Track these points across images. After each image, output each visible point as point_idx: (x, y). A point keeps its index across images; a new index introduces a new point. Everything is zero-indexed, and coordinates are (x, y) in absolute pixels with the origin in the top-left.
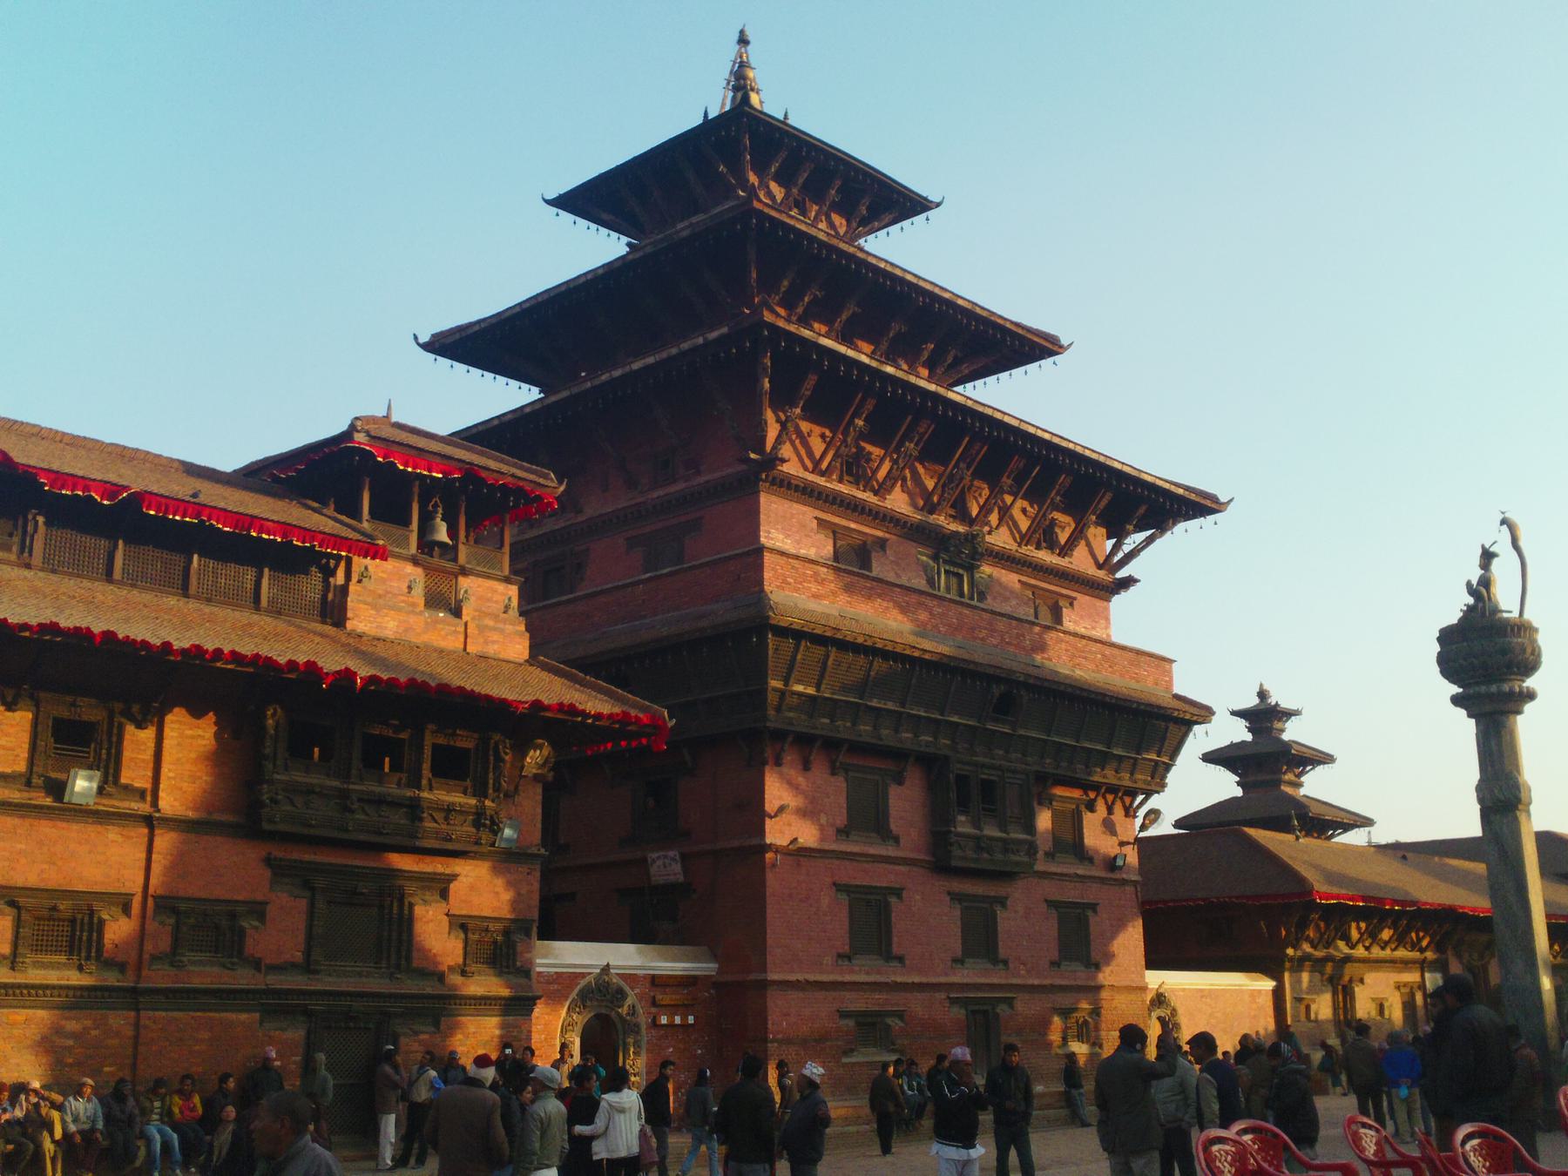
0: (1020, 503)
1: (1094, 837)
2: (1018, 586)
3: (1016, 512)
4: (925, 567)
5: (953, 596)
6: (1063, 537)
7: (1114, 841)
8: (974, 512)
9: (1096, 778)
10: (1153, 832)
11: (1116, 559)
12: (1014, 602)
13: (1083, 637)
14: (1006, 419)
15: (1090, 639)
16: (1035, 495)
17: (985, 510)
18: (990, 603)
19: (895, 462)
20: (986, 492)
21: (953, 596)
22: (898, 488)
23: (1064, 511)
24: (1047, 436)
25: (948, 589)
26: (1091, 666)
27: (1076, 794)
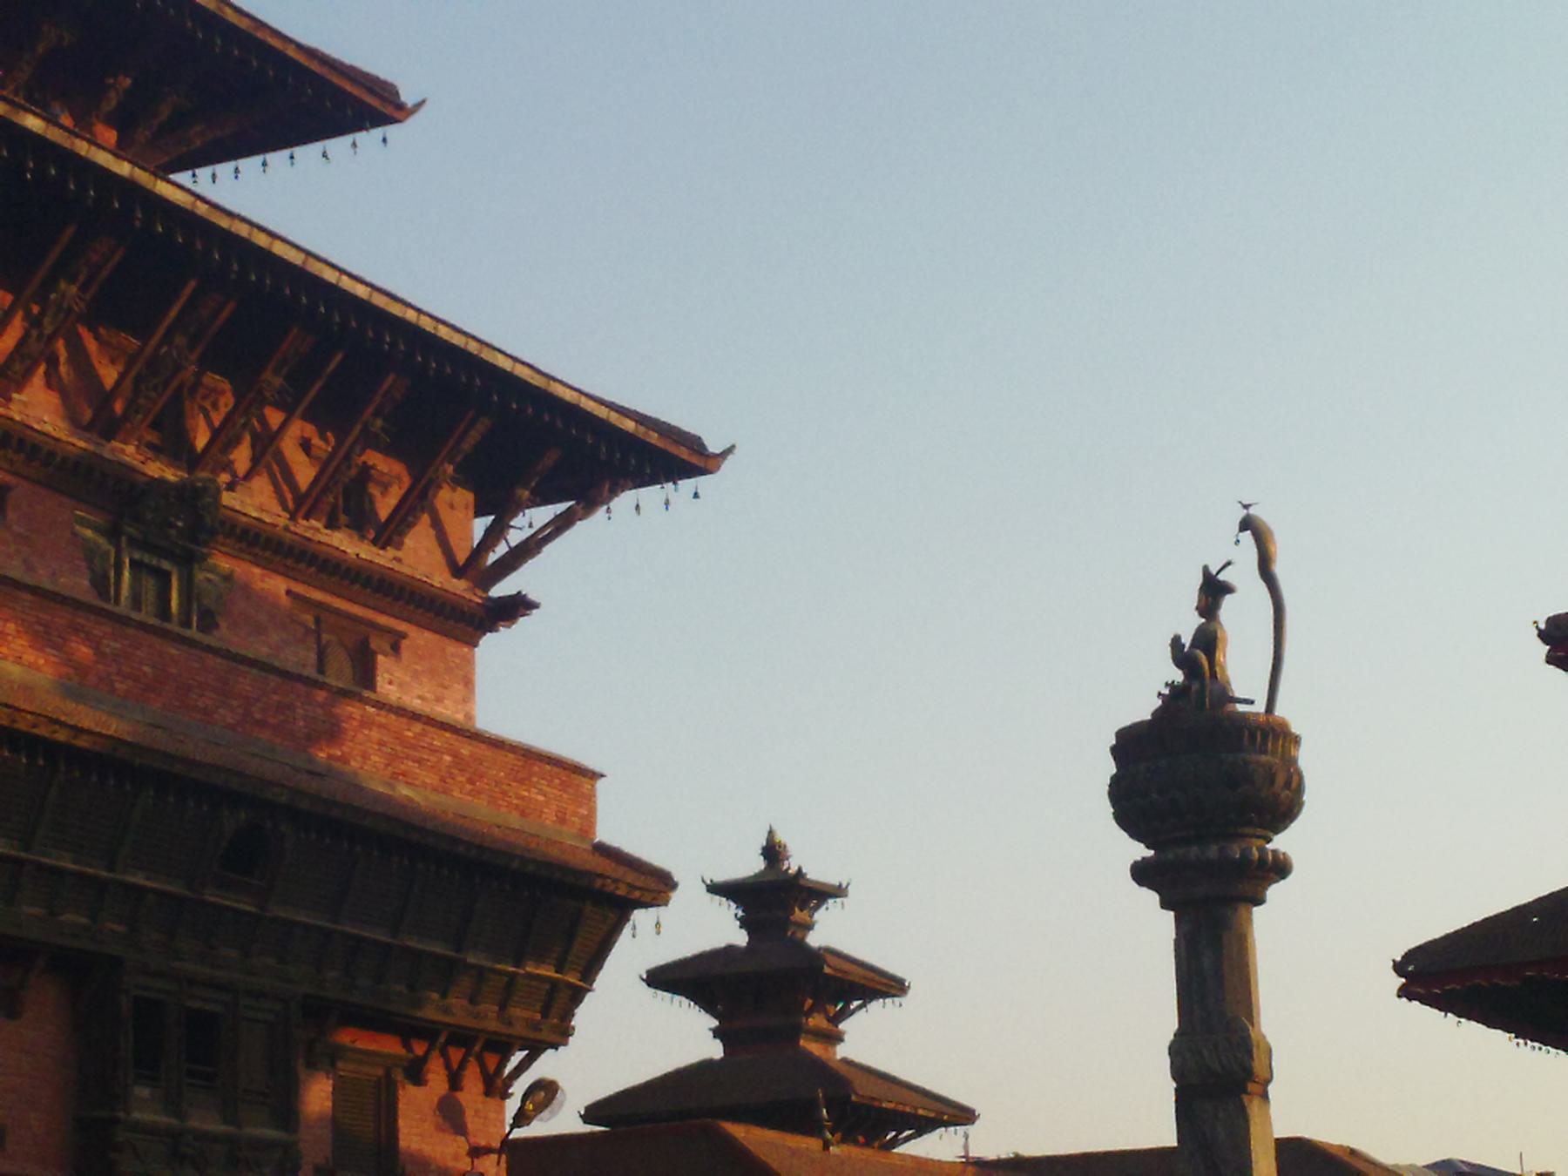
0: (298, 428)
1: (416, 1132)
2: (285, 601)
3: (289, 447)
4: (90, 553)
5: (147, 616)
6: (385, 506)
7: (461, 1144)
8: (201, 441)
9: (430, 1013)
10: (538, 1129)
11: (492, 558)
12: (275, 637)
13: (415, 716)
14: (279, 249)
15: (430, 721)
16: (332, 414)
17: (224, 438)
18: (224, 636)
19: (34, 322)
20: (227, 402)
21: (147, 616)
22: (38, 379)
23: (389, 451)
24: (361, 291)
25: (136, 602)
26: (431, 779)
27: (390, 1046)
